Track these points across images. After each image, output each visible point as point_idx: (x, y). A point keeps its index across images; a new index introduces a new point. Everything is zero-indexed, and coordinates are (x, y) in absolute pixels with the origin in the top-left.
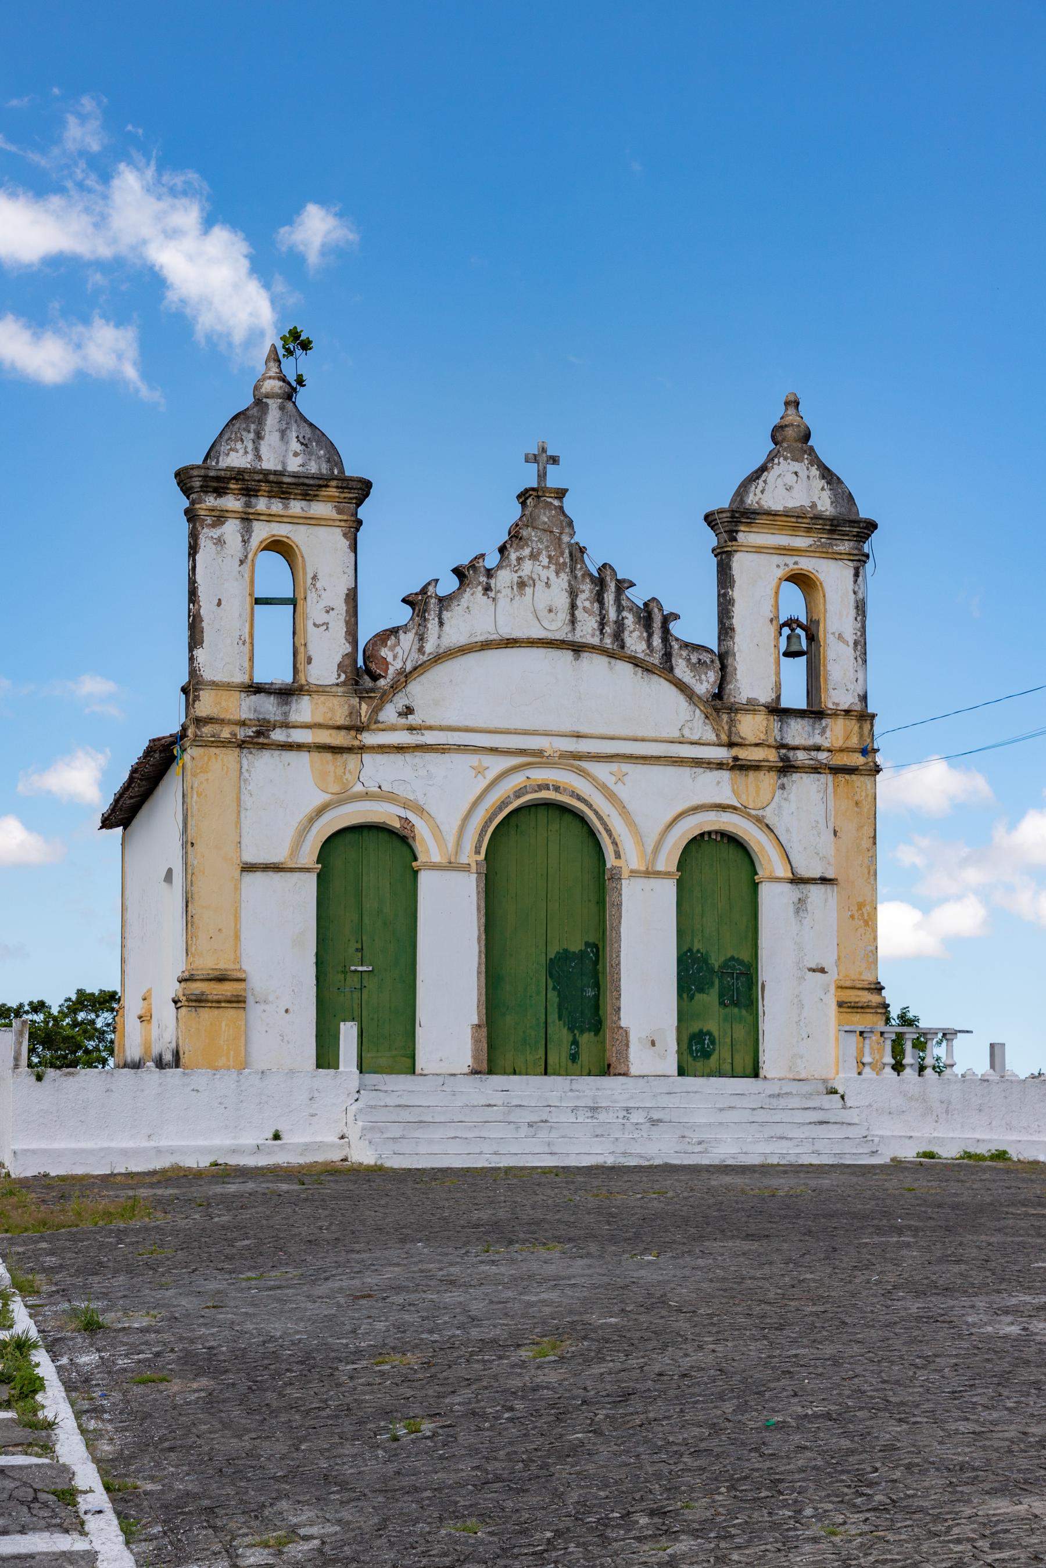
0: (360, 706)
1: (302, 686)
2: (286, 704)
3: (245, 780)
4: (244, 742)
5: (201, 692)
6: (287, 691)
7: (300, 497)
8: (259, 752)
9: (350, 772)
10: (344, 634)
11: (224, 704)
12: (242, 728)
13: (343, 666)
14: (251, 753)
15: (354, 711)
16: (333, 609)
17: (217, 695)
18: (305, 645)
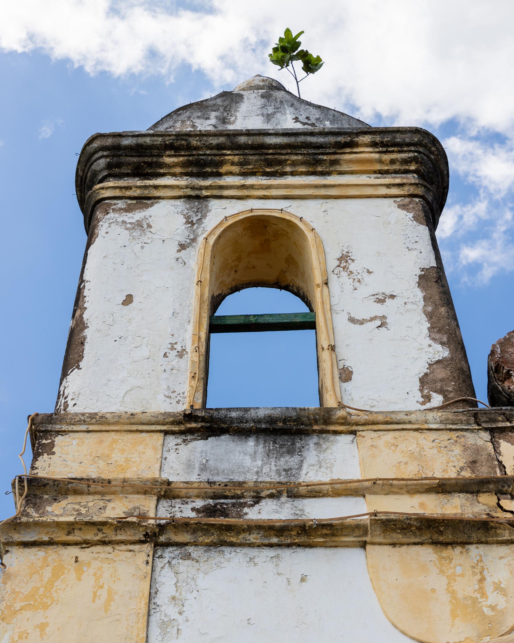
0: (496, 448)
1: (329, 411)
2: (291, 452)
3: (164, 625)
4: (162, 528)
5: (59, 440)
6: (289, 425)
7: (303, 169)
8: (213, 553)
9: (498, 587)
10: (427, 331)
11: (117, 457)
12: (164, 504)
13: (435, 381)
14: (188, 557)
15: (483, 457)
16: (392, 297)
17: (101, 442)
18: (332, 348)
